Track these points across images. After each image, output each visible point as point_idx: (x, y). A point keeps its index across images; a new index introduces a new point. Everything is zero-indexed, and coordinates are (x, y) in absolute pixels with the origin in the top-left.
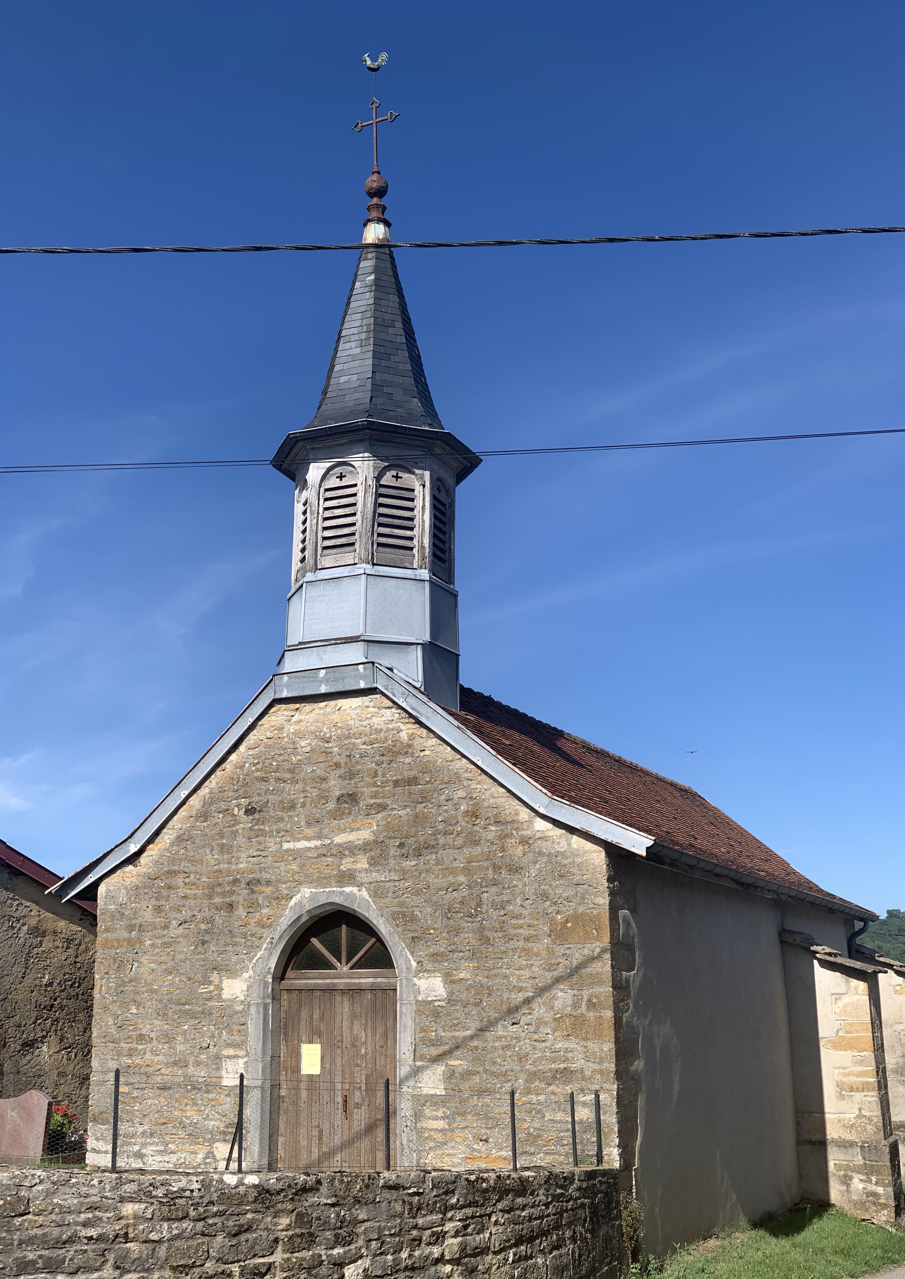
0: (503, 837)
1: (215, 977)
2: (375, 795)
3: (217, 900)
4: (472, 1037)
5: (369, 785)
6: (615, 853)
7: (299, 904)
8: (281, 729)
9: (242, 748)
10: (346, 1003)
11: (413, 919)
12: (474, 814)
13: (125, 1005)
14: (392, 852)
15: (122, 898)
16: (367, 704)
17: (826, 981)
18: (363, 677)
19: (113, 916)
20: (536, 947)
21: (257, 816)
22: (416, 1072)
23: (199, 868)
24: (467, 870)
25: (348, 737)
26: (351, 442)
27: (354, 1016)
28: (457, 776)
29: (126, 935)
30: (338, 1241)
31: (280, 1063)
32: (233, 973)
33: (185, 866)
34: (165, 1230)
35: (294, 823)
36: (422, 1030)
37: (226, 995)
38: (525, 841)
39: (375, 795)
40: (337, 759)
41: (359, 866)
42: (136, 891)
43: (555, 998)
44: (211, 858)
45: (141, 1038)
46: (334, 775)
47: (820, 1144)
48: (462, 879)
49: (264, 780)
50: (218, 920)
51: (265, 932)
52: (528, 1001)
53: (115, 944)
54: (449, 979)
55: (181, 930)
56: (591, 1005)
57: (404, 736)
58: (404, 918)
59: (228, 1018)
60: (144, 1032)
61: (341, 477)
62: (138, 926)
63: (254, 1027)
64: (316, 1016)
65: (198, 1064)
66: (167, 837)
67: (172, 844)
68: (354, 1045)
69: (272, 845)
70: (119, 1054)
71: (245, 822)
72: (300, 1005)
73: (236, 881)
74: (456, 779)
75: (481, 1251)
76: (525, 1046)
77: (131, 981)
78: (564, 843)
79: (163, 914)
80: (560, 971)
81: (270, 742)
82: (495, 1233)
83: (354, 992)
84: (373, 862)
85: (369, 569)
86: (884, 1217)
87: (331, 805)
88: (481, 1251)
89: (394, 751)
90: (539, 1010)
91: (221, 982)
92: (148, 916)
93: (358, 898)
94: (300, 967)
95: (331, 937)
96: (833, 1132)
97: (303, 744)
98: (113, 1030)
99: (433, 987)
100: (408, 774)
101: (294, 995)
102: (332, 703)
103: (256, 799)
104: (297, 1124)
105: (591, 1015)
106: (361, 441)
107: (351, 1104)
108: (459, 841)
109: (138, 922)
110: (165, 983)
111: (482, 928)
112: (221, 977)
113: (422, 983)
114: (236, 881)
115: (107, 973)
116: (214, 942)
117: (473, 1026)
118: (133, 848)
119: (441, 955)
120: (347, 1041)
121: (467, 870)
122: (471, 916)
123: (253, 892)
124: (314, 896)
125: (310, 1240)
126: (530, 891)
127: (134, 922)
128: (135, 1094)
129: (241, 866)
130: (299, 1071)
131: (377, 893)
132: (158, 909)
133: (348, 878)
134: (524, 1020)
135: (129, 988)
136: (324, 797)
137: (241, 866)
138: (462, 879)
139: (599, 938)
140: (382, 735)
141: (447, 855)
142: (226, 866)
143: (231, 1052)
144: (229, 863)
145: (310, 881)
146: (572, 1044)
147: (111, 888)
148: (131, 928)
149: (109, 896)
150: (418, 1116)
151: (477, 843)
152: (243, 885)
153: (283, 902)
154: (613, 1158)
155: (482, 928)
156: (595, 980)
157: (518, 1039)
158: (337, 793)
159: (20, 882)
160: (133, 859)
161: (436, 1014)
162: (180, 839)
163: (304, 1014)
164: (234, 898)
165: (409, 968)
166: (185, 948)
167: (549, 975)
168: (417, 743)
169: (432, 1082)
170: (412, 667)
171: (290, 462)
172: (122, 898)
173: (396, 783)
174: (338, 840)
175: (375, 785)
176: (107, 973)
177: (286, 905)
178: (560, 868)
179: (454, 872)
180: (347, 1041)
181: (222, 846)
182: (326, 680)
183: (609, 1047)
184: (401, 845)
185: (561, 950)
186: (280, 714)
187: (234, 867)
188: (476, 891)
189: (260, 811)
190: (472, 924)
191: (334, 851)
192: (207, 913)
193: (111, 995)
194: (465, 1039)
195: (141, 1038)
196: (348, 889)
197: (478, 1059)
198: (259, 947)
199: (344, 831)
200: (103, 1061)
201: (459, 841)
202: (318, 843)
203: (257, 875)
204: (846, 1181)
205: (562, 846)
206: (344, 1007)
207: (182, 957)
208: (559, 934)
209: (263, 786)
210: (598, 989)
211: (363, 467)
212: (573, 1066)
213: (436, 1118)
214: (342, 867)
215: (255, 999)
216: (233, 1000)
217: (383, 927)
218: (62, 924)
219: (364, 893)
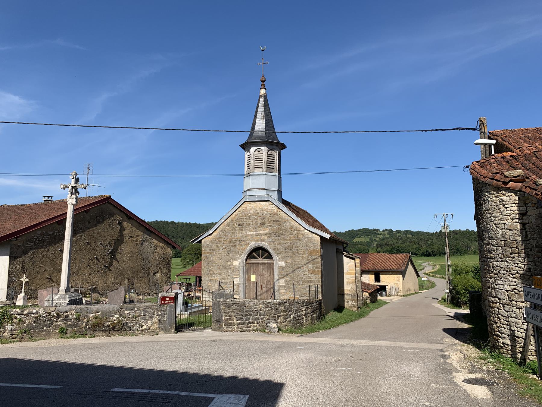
2: (269, 223)
6: (322, 238)
11: (278, 250)
12: (291, 228)
13: (210, 266)
15: (208, 243)
17: (346, 260)
20: (305, 256)
24: (290, 240)
27: (263, 269)
28: (288, 220)
30: (290, 311)
31: (247, 279)
32: (236, 260)
34: (266, 309)
38: (303, 234)
39: (269, 223)
44: (230, 235)
45: (214, 273)
46: (259, 218)
47: (343, 294)
52: (303, 266)
54: (286, 262)
56: (316, 268)
57: (275, 211)
58: (276, 249)
59: (235, 269)
63: (241, 271)
65: (228, 279)
66: (219, 230)
71: (238, 228)
75: (308, 314)
82: (309, 311)
83: (263, 264)
84: (269, 237)
85: (266, 173)
86: (355, 309)
87: (259, 225)
88: (308, 314)
92: (215, 247)
94: (250, 259)
95: (258, 253)
96: (345, 292)
99: (282, 263)
104: (250, 291)
108: (288, 234)
110: (219, 262)
113: (280, 263)
116: (231, 252)
118: (211, 232)
120: (262, 274)
121: (290, 240)
125: (286, 311)
130: (250, 280)
131: (269, 244)
132: (217, 246)
133: (263, 240)
136: (257, 223)
145: (253, 241)
146: (312, 275)
148: (210, 250)
154: (320, 297)
159: (152, 234)
161: (283, 269)
162: (222, 231)
163: (252, 268)
166: (224, 254)
168: (278, 213)
169: (282, 282)
170: (275, 195)
171: (245, 146)
173: (274, 221)
174: (260, 232)
178: (310, 240)
179: (287, 240)
180: (262, 274)
182: (258, 198)
183: (320, 276)
185: (310, 257)
186: (246, 204)
190: (291, 250)
192: (229, 247)
195: (214, 273)
197: (292, 278)
200: (205, 279)
201: (288, 234)
204: (348, 302)
205: (311, 236)
206: (261, 267)
208: (310, 253)
209: (242, 220)
211: (264, 149)
215: (241, 265)
217: (271, 251)
218: (161, 244)
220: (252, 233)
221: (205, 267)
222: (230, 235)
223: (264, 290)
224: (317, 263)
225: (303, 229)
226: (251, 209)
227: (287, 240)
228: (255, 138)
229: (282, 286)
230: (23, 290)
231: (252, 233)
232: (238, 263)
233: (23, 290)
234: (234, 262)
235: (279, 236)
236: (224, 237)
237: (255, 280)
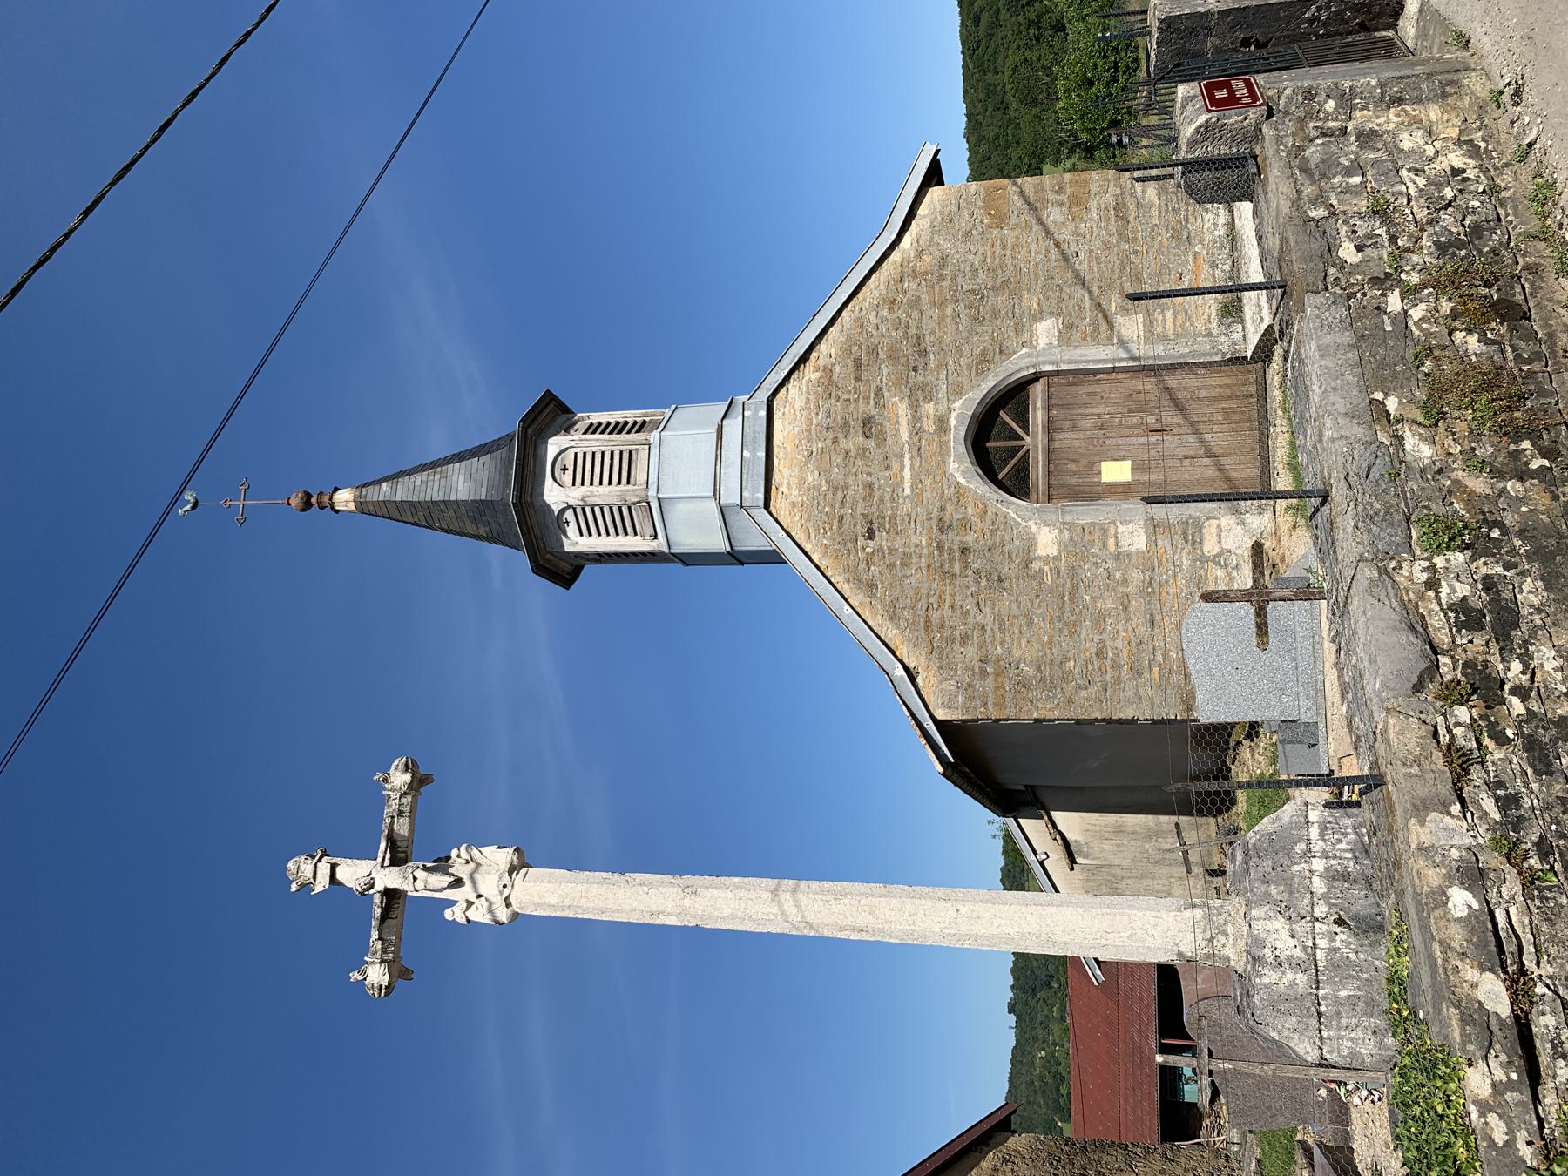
0: (914, 275)
1: (1035, 566)
3: (957, 567)
4: (1090, 292)
5: (857, 407)
7: (963, 473)
8: (794, 505)
9: (808, 548)
10: (1063, 435)
11: (984, 353)
12: (892, 303)
13: (1066, 676)
14: (920, 378)
15: (950, 686)
18: (756, 412)
19: (971, 698)
20: (1011, 241)
21: (875, 527)
22: (1122, 343)
23: (924, 591)
25: (810, 431)
27: (1074, 428)
29: (990, 679)
32: (1032, 543)
36: (1084, 339)
37: (1053, 551)
38: (919, 254)
39: (867, 399)
40: (829, 441)
41: (931, 412)
43: (1055, 222)
44: (915, 577)
45: (1100, 654)
48: (949, 310)
51: (991, 510)
52: (1057, 245)
54: (1039, 316)
55: (987, 610)
58: (982, 363)
59: (1077, 545)
60: (1093, 650)
61: (565, 469)
63: (1085, 515)
64: (1073, 467)
65: (1125, 581)
66: (890, 633)
67: (898, 626)
68: (1101, 427)
69: (906, 507)
70: (1118, 681)
71: (882, 539)
72: (1063, 485)
73: (939, 547)
74: (859, 323)
76: (1096, 244)
77: (1039, 670)
80: (1030, 218)
83: (1051, 428)
84: (929, 397)
87: (872, 444)
89: (828, 384)
90: (1065, 235)
91: (1040, 558)
92: (971, 653)
93: (961, 411)
98: (1093, 690)
99: (1045, 331)
100: (851, 368)
102: (776, 450)
105: (1069, 191)
106: (536, 446)
107: (1157, 426)
108: (916, 315)
109: (977, 664)
111: (993, 288)
113: (1042, 341)
117: (1079, 291)
118: (899, 672)
119: (1017, 325)
121: (942, 305)
122: (982, 299)
123: (950, 525)
124: (958, 459)
126: (962, 248)
128: (1160, 659)
131: (957, 392)
132: (965, 639)
133: (942, 423)
134: (1074, 248)
135: (1047, 673)
136: (863, 453)
138: (949, 310)
139: (1004, 188)
141: (927, 325)
143: (1111, 541)
145: (943, 464)
148: (984, 674)
150: (1164, 338)
151: (918, 299)
152: (944, 537)
155: (993, 288)
156: (1040, 189)
157: (1091, 251)
160: (913, 679)
161: (1070, 326)
162: (893, 617)
163: (1072, 480)
164: (956, 548)
165: (1029, 355)
166: (1006, 604)
167: (1036, 228)
168: (821, 362)
169: (1131, 326)
173: (857, 379)
174: (905, 436)
175: (857, 401)
179: (942, 318)
181: (903, 565)
184: (915, 369)
185: (1014, 219)
187: (925, 551)
188: (960, 296)
190: (988, 298)
191: (916, 439)
192: (970, 579)
194: (1091, 298)
195: (1100, 654)
196: (953, 422)
198: (1006, 515)
199: (898, 431)
200: (1127, 702)
202: (907, 456)
203: (934, 522)
206: (1065, 438)
207: (1014, 606)
208: (1000, 220)
209: (847, 520)
210: (1048, 186)
212: (1112, 203)
213: (1164, 321)
216: (1059, 543)
217: (989, 383)
218: (984, 1164)
219: (958, 404)
220: (907, 474)
221: (1070, 702)
222: (915, 577)
223: (1171, 418)
224: (1040, 189)
225: (896, 256)
227: (942, 318)
229: (1149, 324)
231: (907, 474)
232: (1043, 532)
234: (1041, 552)
235: (924, 353)
236: (922, 604)
237: (1127, 464)
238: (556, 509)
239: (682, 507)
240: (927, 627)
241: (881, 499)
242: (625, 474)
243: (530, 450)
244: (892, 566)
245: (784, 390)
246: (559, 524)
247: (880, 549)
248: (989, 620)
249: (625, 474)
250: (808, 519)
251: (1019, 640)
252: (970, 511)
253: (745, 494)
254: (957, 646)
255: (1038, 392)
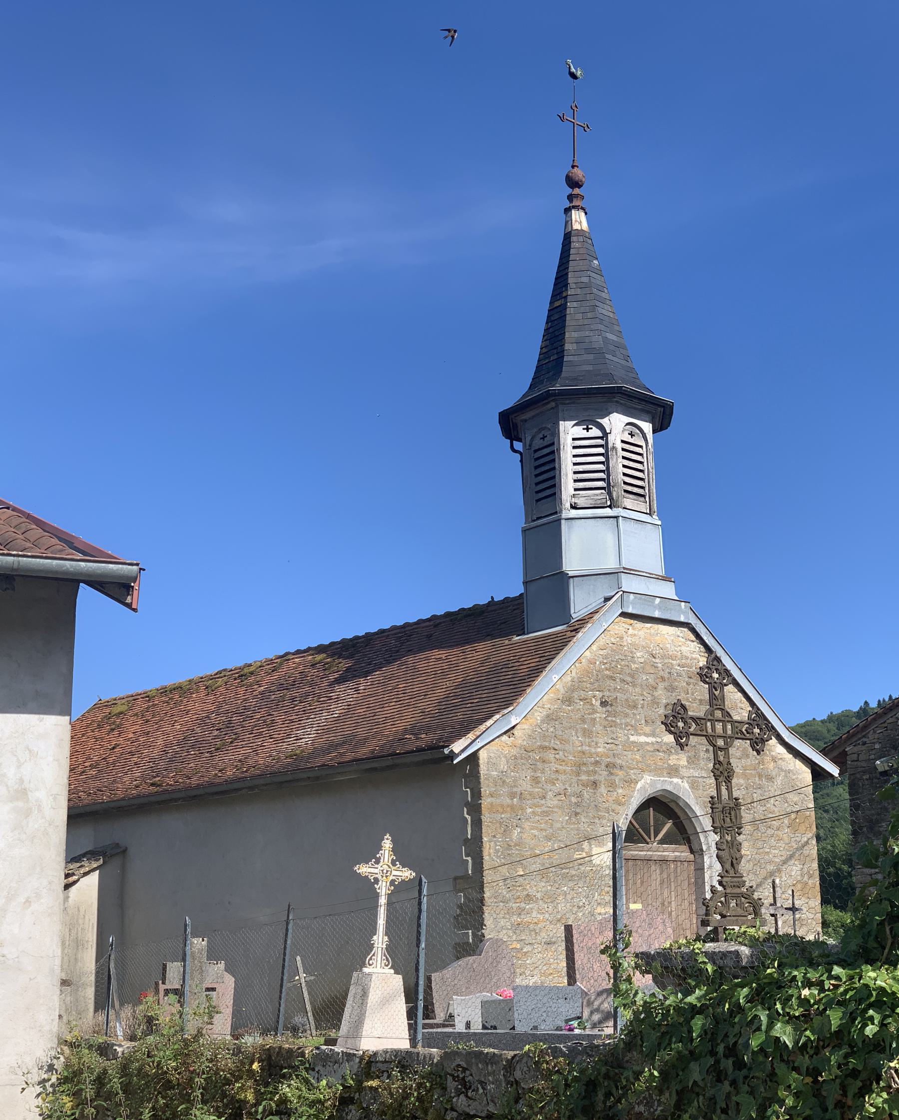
3: (584, 777)
7: (643, 788)
8: (622, 638)
14: (702, 754)
16: (678, 633)
23: (568, 747)
26: (642, 410)
33: (557, 744)
35: (639, 721)
38: (774, 760)
40: (661, 673)
42: (516, 761)
44: (577, 740)
49: (612, 678)
50: (586, 796)
51: (620, 809)
53: (500, 810)
61: (632, 435)
62: (519, 793)
67: (543, 721)
69: (621, 735)
71: (601, 714)
77: (516, 845)
78: (792, 764)
79: (540, 785)
81: (614, 647)
83: (664, 861)
91: (591, 849)
97: (639, 654)
101: (631, 863)
102: (656, 626)
103: (607, 693)
106: (648, 412)
109: (517, 790)
112: (590, 845)
114: (597, 763)
115: (494, 836)
123: (612, 774)
127: (515, 790)
129: (599, 750)
131: (694, 785)
132: (536, 780)
133: (674, 771)
137: (599, 750)
140: (689, 661)
142: (587, 748)
144: (589, 746)
147: (492, 755)
148: (512, 795)
149: (491, 764)
152: (603, 767)
153: (632, 785)
158: (664, 701)
166: (561, 818)
172: (503, 766)
176: (494, 836)
177: (635, 788)
181: (584, 730)
182: (659, 607)
187: (593, 750)
189: (611, 705)
191: (664, 748)
192: (577, 789)
193: (498, 857)
196: (675, 780)
202: (654, 740)
206: (655, 873)
207: (558, 825)
214: (670, 762)
219: (686, 785)
220: (643, 739)
226: (636, 647)
228: (575, 380)
230: (380, 940)
231: (643, 739)
233: (380, 940)
238: (605, 422)
239: (610, 539)
240: (543, 748)
241: (626, 715)
242: (629, 488)
243: (650, 407)
244: (583, 720)
245: (693, 637)
246: (587, 422)
247: (595, 711)
248: (550, 803)
249: (629, 488)
250: (613, 650)
251: (537, 828)
252: (620, 791)
253: (632, 596)
254: (529, 773)
255: (680, 852)
